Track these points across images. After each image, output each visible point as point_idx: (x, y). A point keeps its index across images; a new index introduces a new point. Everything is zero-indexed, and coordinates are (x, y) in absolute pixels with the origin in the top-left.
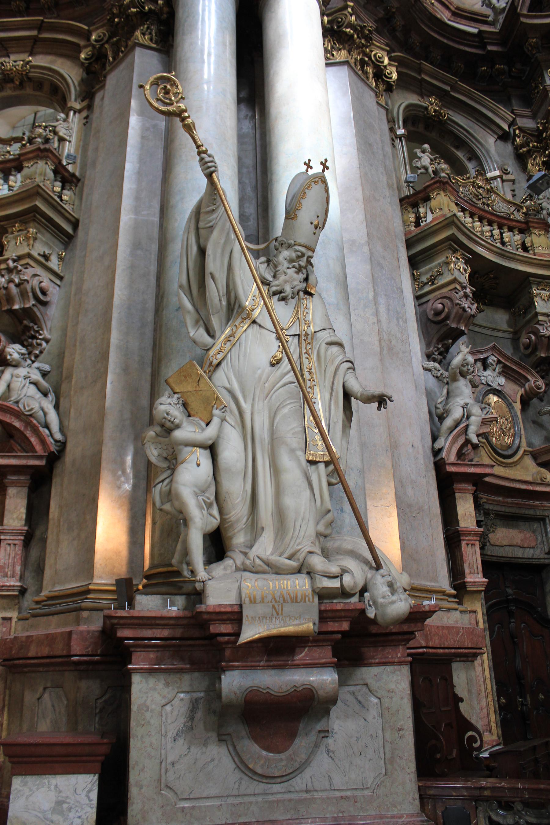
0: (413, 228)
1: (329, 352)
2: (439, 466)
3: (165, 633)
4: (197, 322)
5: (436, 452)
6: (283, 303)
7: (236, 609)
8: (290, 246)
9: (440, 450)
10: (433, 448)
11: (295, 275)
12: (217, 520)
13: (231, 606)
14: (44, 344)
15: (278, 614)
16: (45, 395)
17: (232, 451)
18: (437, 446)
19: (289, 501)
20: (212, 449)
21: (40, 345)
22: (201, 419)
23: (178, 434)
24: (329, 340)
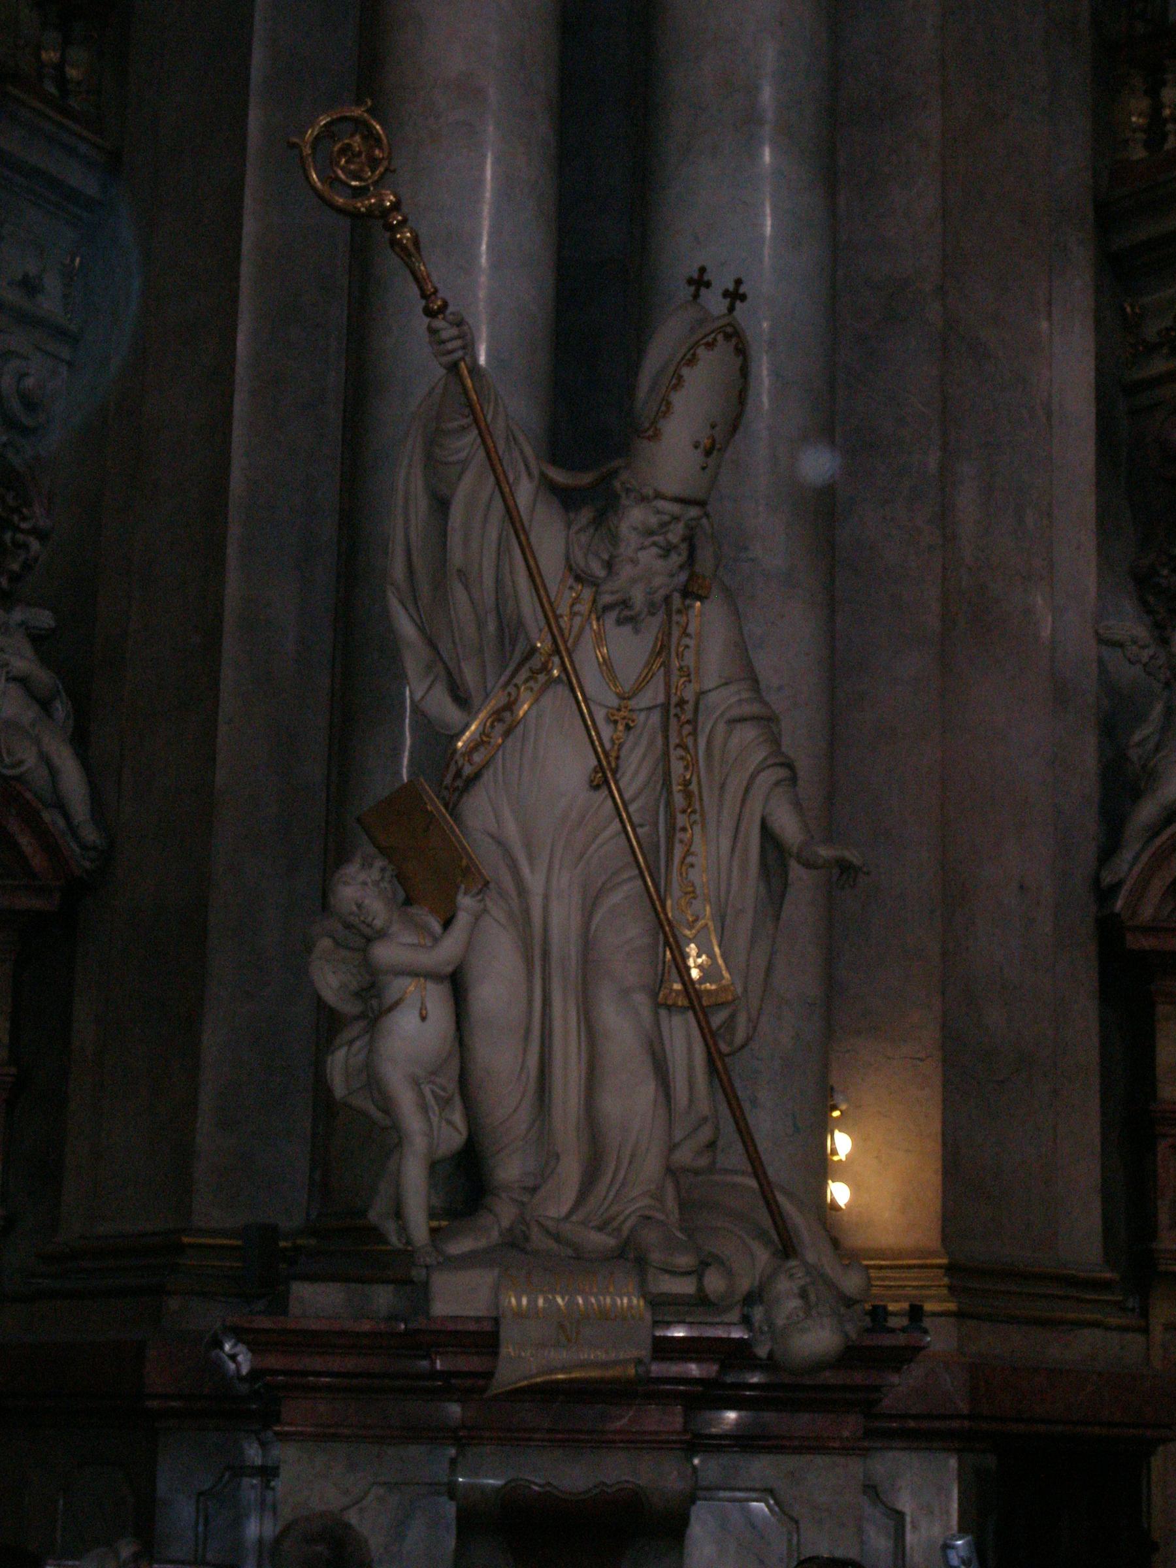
0: (1139, 153)
1: (735, 741)
2: (1109, 931)
3: (350, 1364)
4: (429, 668)
5: (1104, 894)
6: (627, 630)
7: (487, 1326)
8: (644, 499)
9: (1116, 887)
10: (1097, 880)
11: (659, 564)
12: (460, 1133)
13: (478, 1319)
14: (35, 545)
15: (569, 1341)
16: (45, 705)
17: (498, 989)
18: (1107, 879)
19: (611, 1105)
20: (457, 984)
21: (25, 546)
22: (433, 911)
23: (385, 953)
24: (736, 712)
